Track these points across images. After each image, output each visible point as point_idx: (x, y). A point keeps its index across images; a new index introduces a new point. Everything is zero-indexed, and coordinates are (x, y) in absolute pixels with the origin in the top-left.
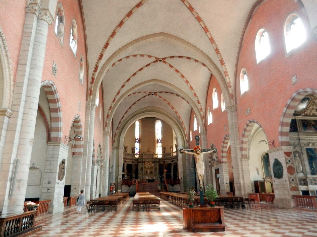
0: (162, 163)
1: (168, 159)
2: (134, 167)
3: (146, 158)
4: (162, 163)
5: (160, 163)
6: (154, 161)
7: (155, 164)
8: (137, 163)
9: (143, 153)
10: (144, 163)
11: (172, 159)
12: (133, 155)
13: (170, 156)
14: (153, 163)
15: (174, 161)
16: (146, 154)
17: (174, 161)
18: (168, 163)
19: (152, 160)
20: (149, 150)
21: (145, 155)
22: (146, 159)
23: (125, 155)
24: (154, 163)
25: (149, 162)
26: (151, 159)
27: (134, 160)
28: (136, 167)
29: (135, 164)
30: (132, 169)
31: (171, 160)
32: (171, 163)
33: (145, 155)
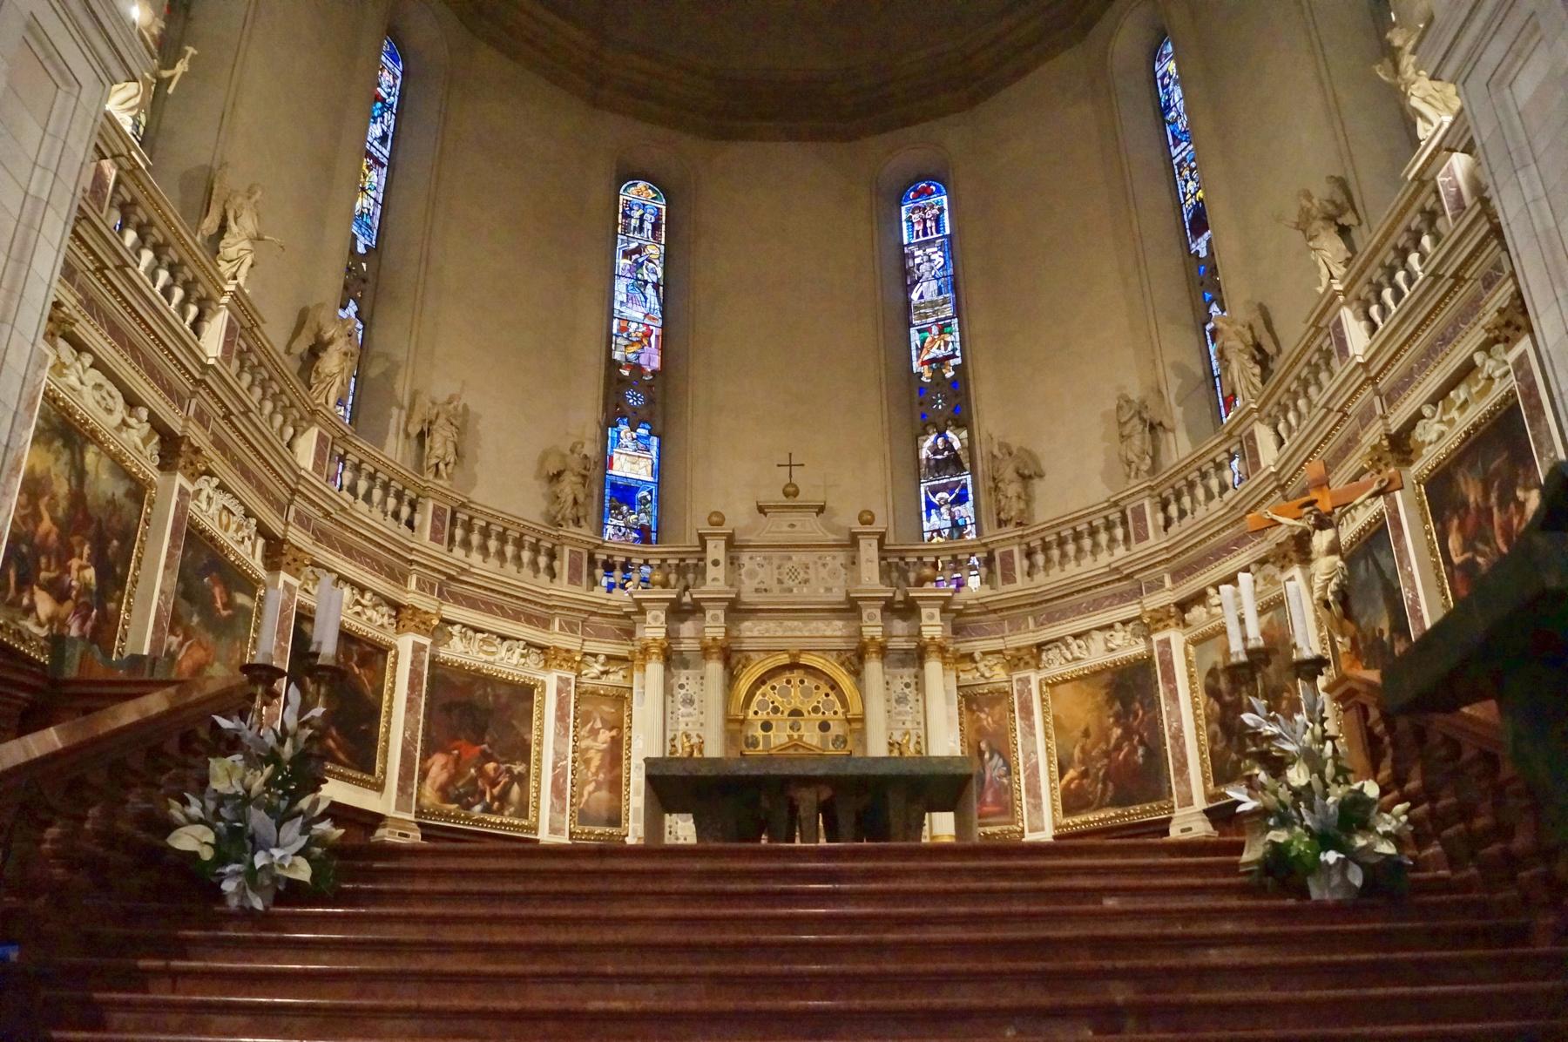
0: (999, 675)
1: (1096, 605)
2: (561, 733)
3: (749, 596)
4: (1000, 675)
5: (967, 678)
6: (873, 628)
7: (898, 686)
8: (616, 678)
9: (705, 528)
10: (715, 668)
11: (1156, 586)
12: (552, 556)
13: (1120, 551)
14: (857, 674)
15: (1200, 597)
16: (754, 539)
17: (1200, 597)
18: (1096, 654)
19: (835, 630)
20: (791, 491)
21: (745, 557)
22: (753, 612)
23: (410, 524)
24: (874, 668)
25: (793, 666)
26: (835, 612)
27: (569, 627)
28: (605, 736)
29: (583, 696)
30: (522, 751)
31: (1166, 597)
32: (1138, 649)
33: (733, 562)
